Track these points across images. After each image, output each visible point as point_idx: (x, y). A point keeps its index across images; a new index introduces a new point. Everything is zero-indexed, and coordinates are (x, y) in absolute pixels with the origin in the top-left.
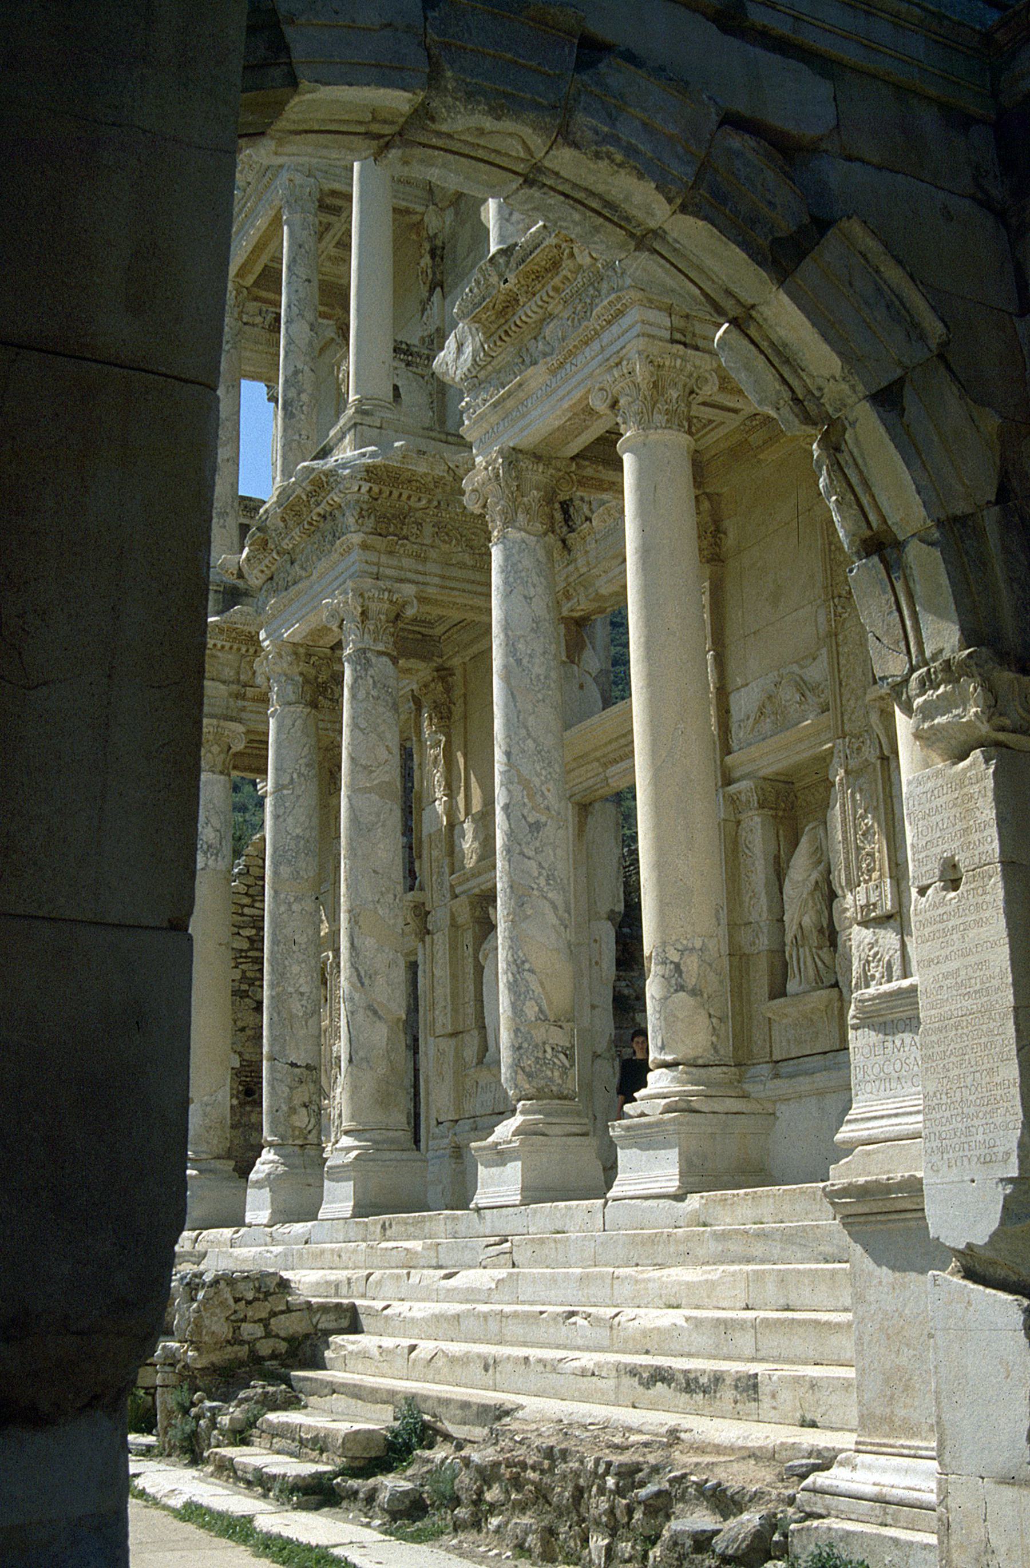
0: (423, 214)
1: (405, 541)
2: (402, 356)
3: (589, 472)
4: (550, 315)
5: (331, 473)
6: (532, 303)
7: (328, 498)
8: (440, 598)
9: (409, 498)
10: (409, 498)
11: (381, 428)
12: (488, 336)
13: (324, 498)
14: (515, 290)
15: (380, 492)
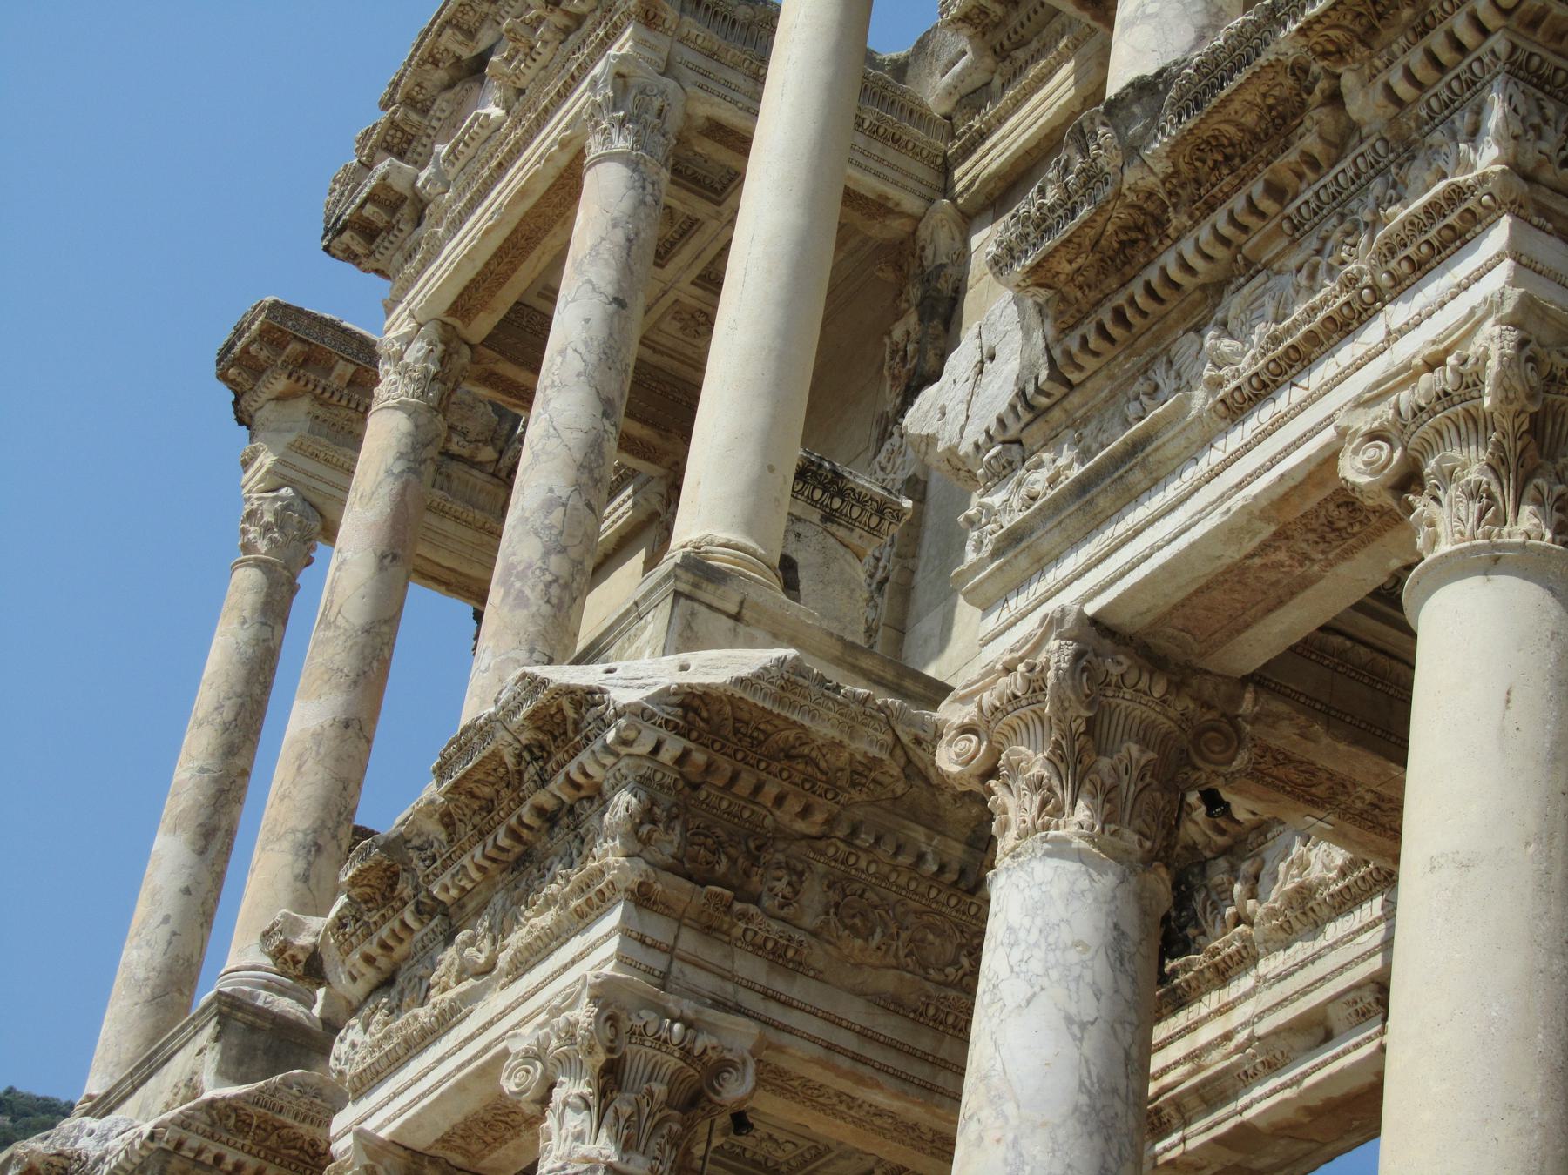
0: (919, 219)
1: (753, 909)
2: (818, 494)
3: (1284, 736)
4: (1249, 264)
5: (586, 698)
6: (1204, 233)
7: (572, 768)
8: (816, 1074)
9: (779, 800)
10: (779, 800)
11: (737, 617)
12: (1064, 331)
13: (561, 765)
14: (1162, 194)
15: (709, 768)
